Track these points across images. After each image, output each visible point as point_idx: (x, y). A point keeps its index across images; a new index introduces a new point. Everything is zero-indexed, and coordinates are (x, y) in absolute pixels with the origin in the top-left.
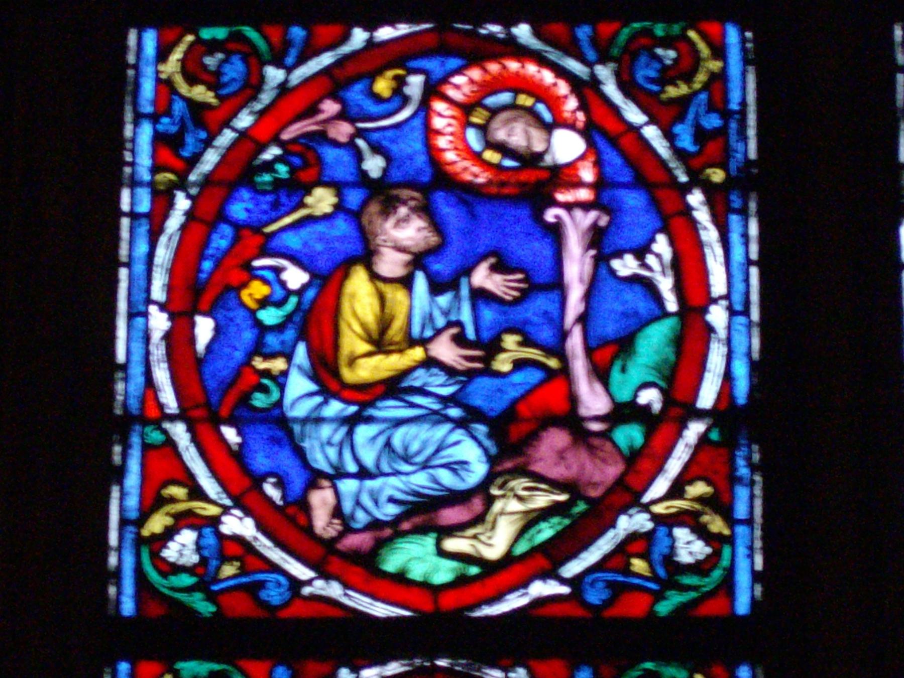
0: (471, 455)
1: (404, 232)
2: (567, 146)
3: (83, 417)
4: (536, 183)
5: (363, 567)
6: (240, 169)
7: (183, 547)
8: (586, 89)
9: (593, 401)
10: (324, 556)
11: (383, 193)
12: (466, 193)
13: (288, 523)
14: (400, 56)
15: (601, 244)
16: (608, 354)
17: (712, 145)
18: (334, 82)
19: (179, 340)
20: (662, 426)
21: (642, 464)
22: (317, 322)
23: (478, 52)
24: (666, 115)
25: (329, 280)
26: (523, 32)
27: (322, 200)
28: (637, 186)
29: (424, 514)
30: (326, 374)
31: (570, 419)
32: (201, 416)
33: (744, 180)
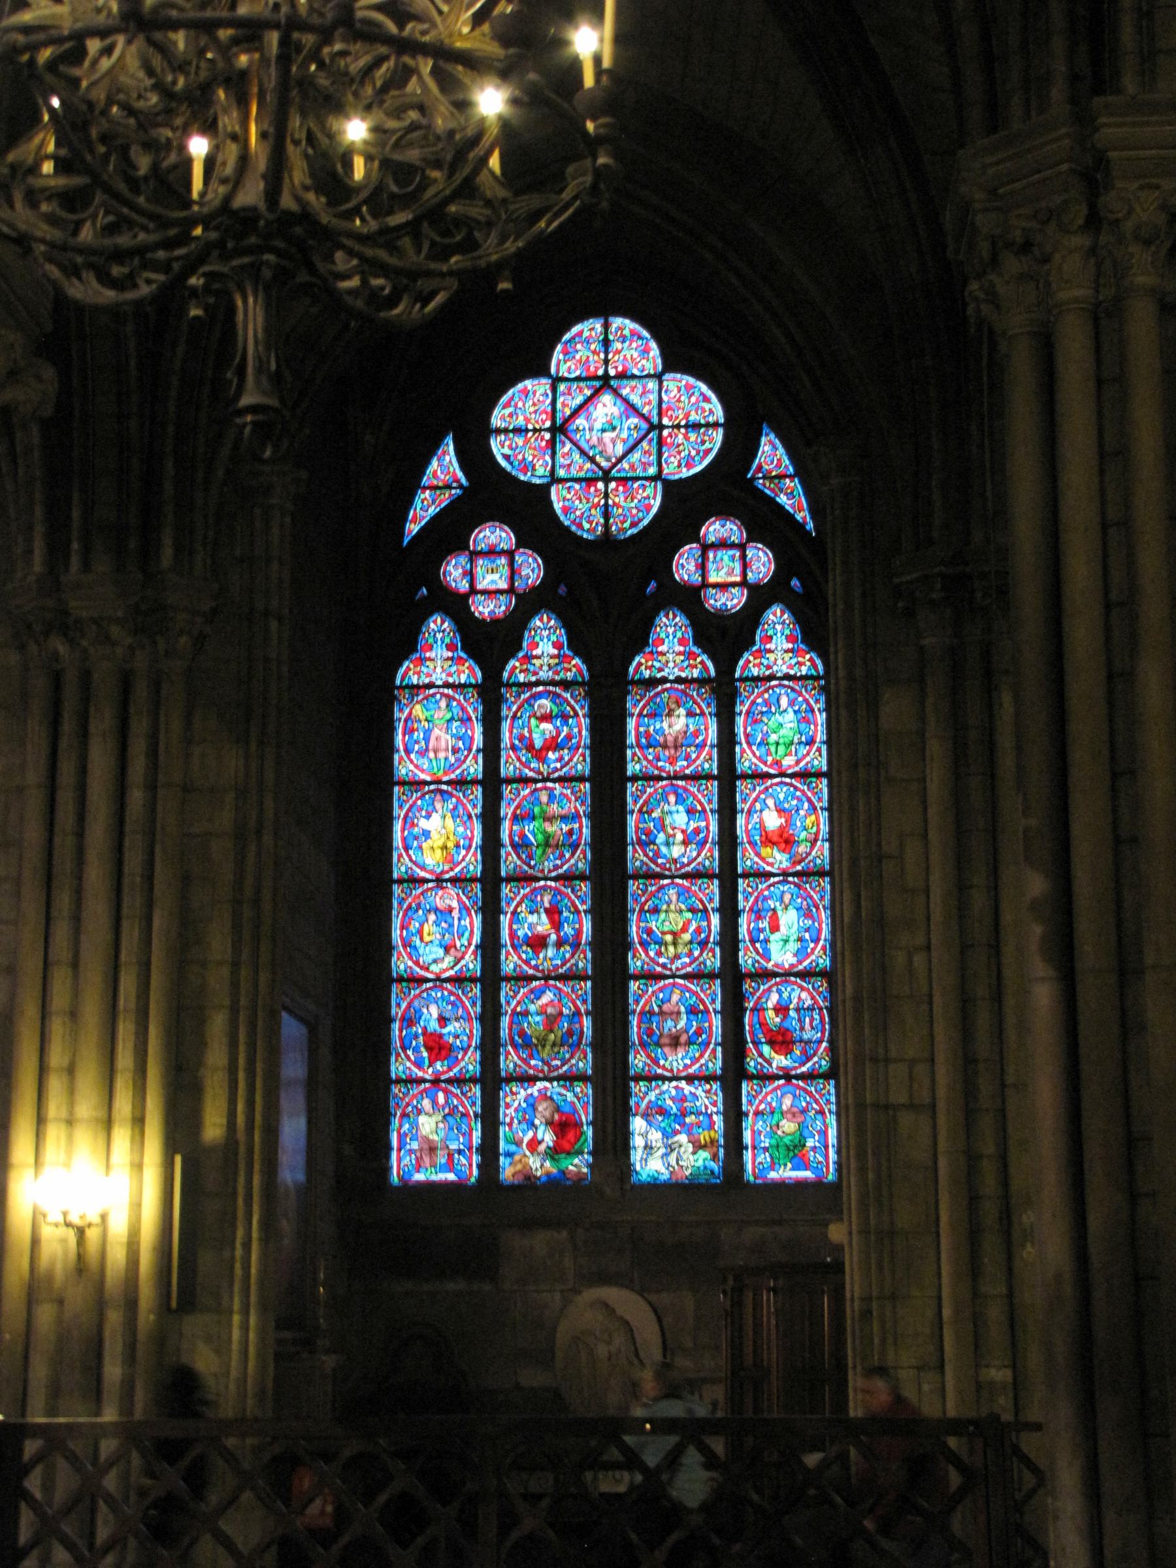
0: (441, 952)
1: (432, 917)
2: (455, 904)
3: (390, 948)
4: (450, 910)
5: (427, 969)
6: (409, 907)
7: (402, 967)
8: (458, 895)
9: (458, 944)
10: (421, 968)
11: (429, 911)
12: (441, 911)
13: (417, 963)
14: (432, 889)
15: (459, 919)
16: (460, 936)
17: (475, 903)
18: (422, 893)
19: (401, 935)
20: (467, 948)
21: (464, 954)
22: (420, 932)
23: (442, 888)
24: (469, 898)
25: (422, 925)
26: (449, 884)
27: (420, 912)
28: (464, 908)
29: (435, 961)
30: (422, 939)
31: (455, 947)
32: (405, 946)
33: (480, 908)
